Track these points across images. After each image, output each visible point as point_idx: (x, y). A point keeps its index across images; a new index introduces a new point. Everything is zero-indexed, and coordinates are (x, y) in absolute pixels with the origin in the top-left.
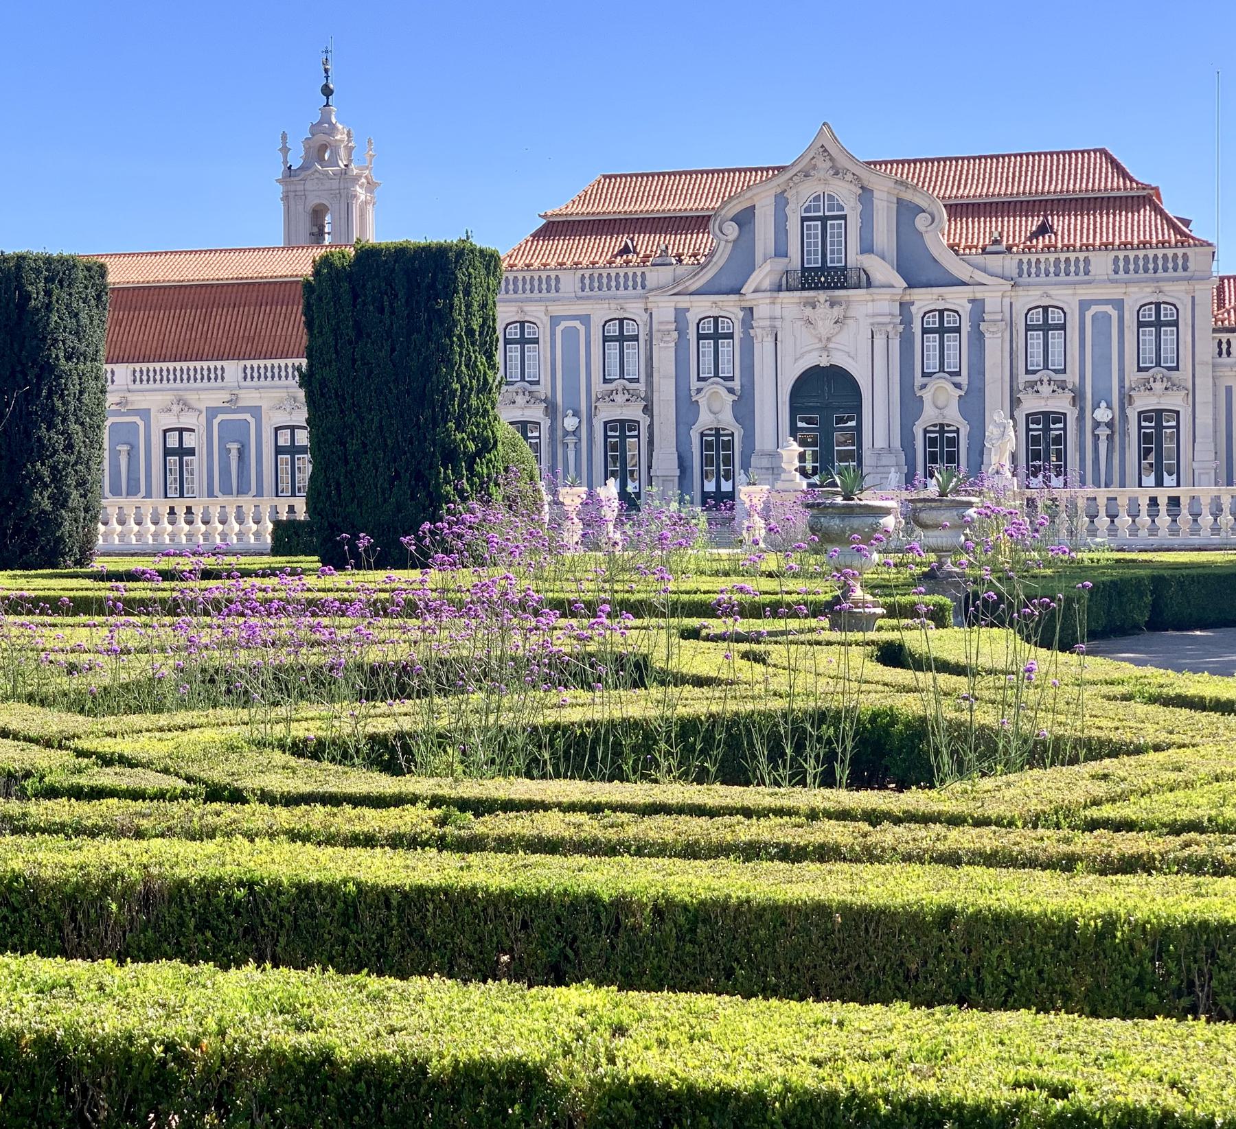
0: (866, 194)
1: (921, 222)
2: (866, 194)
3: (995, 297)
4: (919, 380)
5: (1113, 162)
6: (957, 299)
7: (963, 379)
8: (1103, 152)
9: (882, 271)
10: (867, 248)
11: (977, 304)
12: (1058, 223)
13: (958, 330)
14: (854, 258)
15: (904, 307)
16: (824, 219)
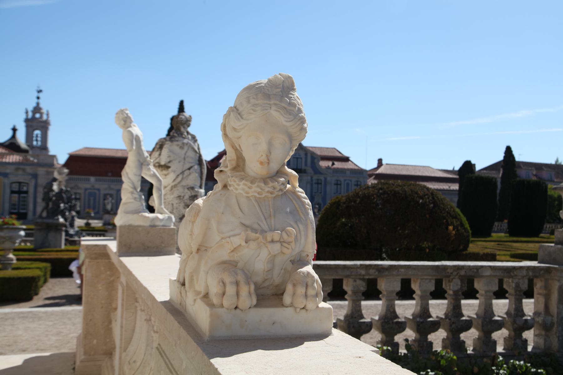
0: (306, 154)
1: (316, 161)
2: (306, 154)
3: (329, 179)
4: (314, 194)
5: (338, 151)
6: (322, 178)
7: (322, 193)
8: (335, 149)
9: (310, 170)
10: (306, 165)
11: (326, 179)
12: (336, 163)
13: (321, 184)
14: (303, 167)
15: (312, 178)
16: (297, 158)
